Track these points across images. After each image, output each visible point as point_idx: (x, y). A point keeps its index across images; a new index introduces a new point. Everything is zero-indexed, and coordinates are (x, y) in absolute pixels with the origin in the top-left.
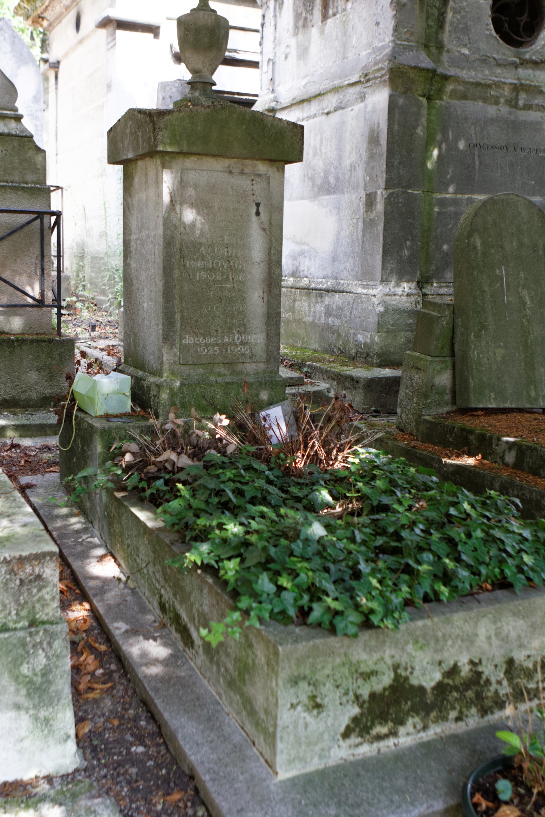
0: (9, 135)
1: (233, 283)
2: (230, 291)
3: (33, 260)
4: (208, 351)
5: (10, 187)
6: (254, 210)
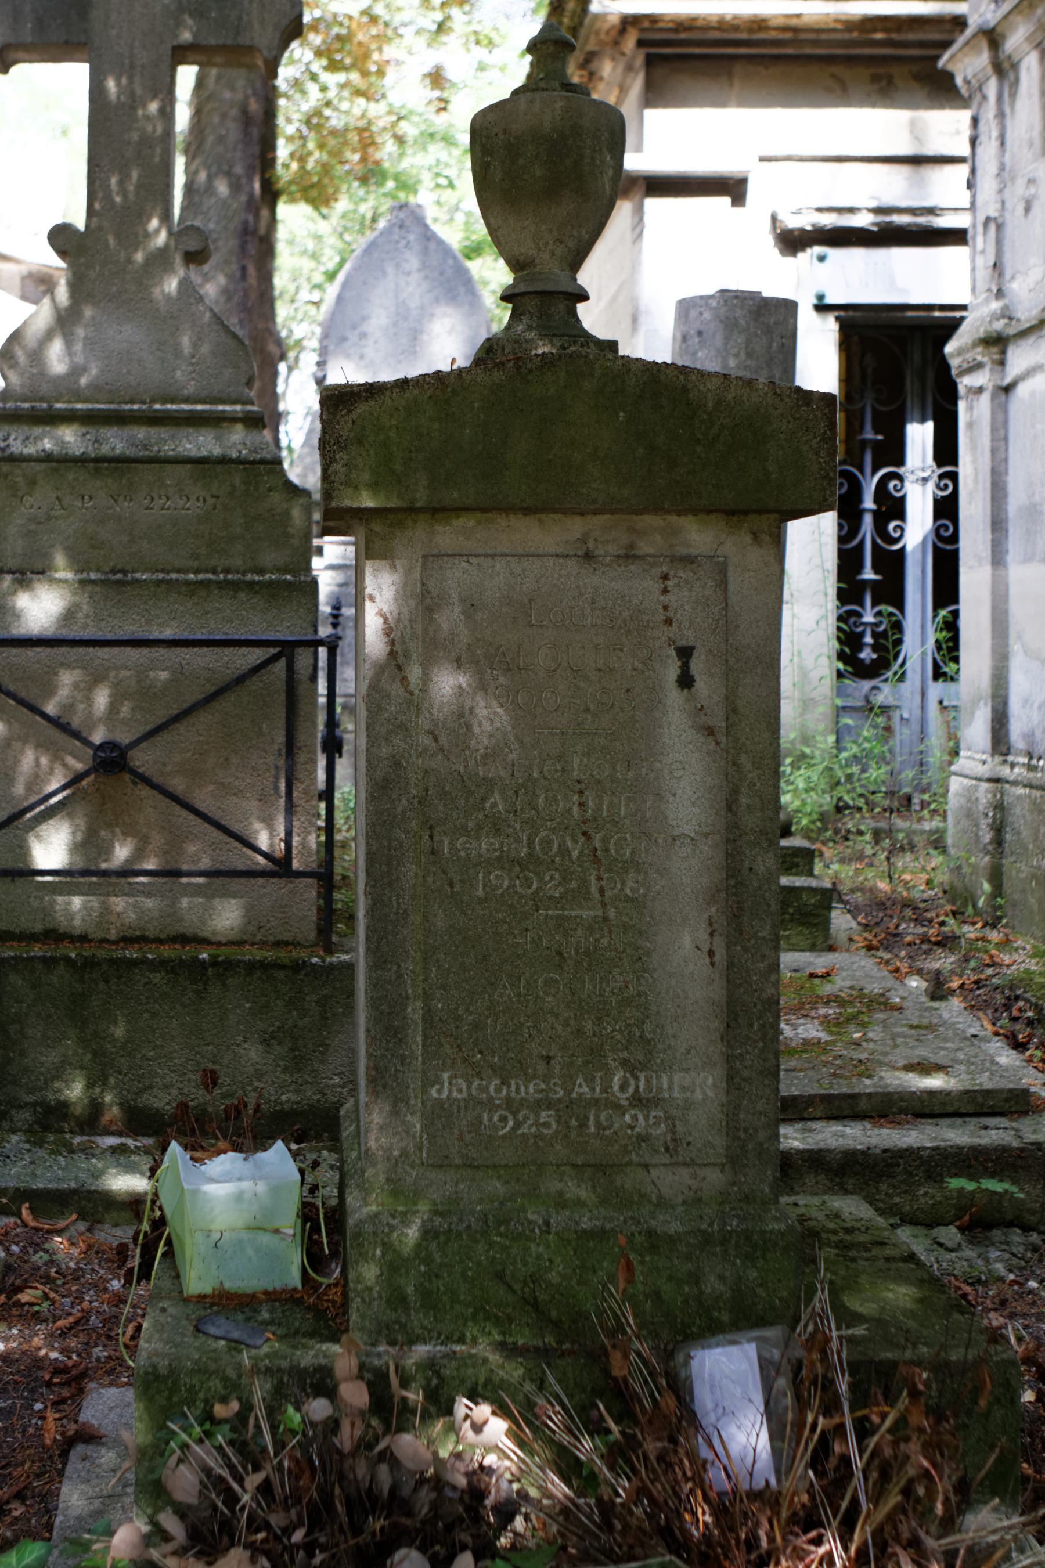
0: (224, 461)
1: (604, 905)
2: (590, 929)
3: (271, 760)
4: (518, 1125)
5: (218, 583)
6: (673, 671)
